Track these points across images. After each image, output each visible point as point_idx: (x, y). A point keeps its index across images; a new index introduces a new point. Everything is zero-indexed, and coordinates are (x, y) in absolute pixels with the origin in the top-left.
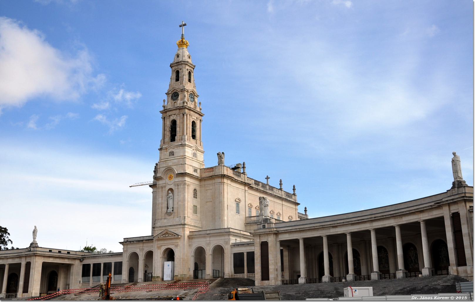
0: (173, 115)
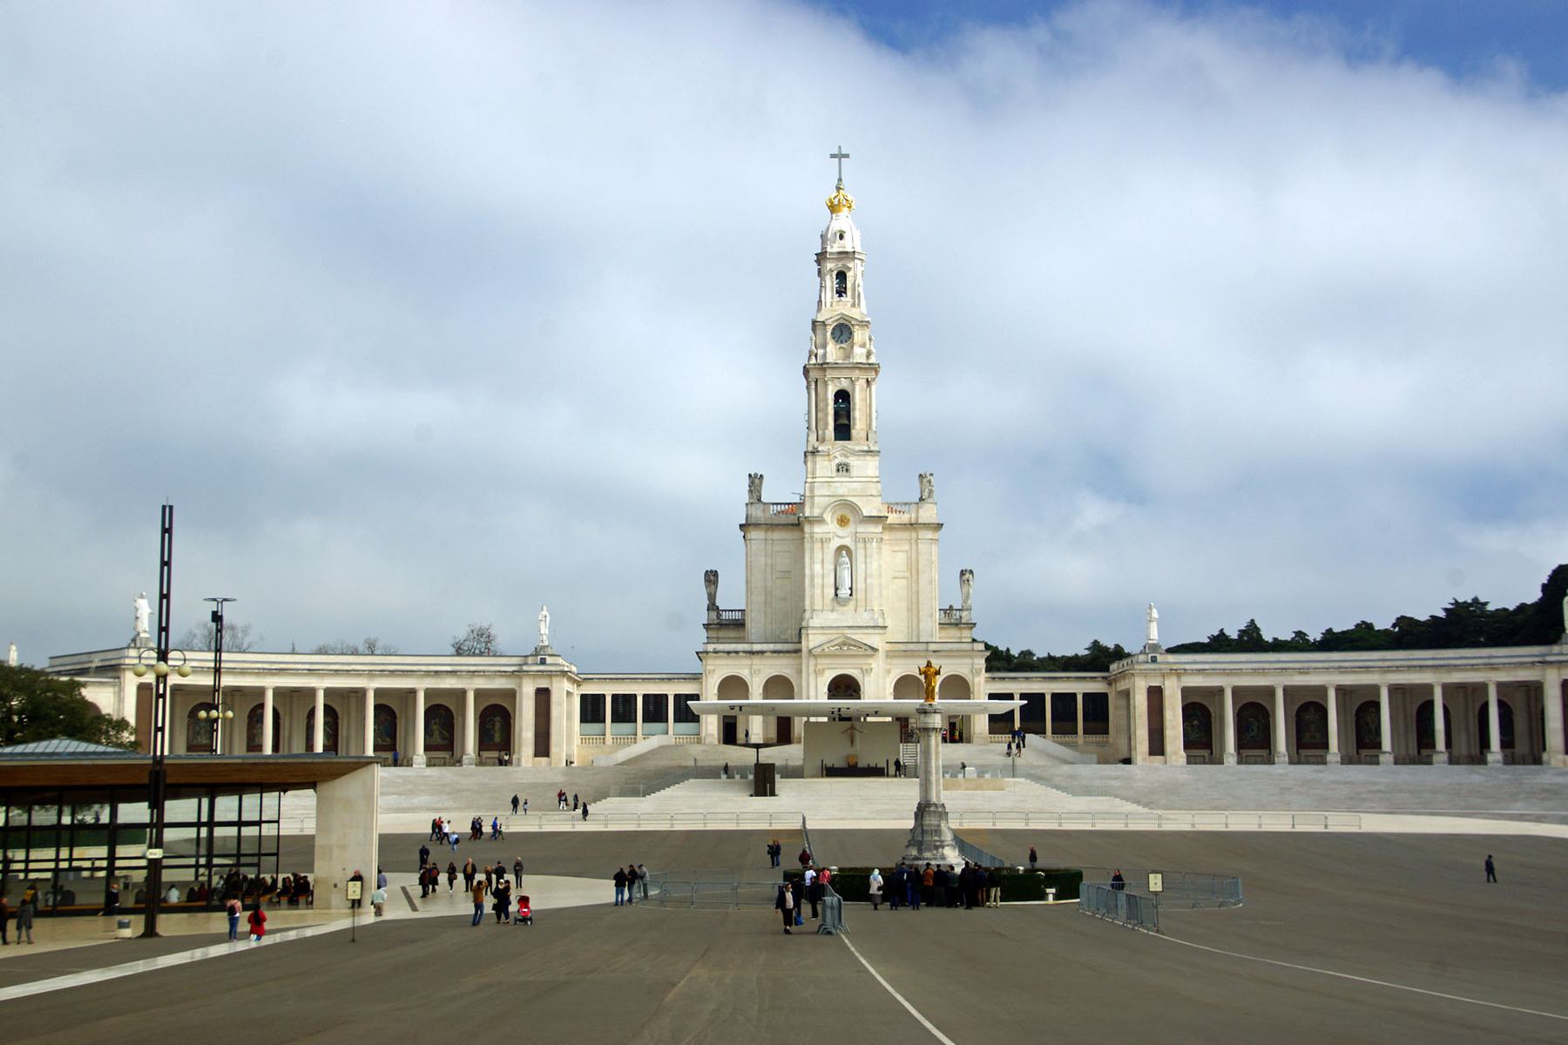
0: (842, 379)
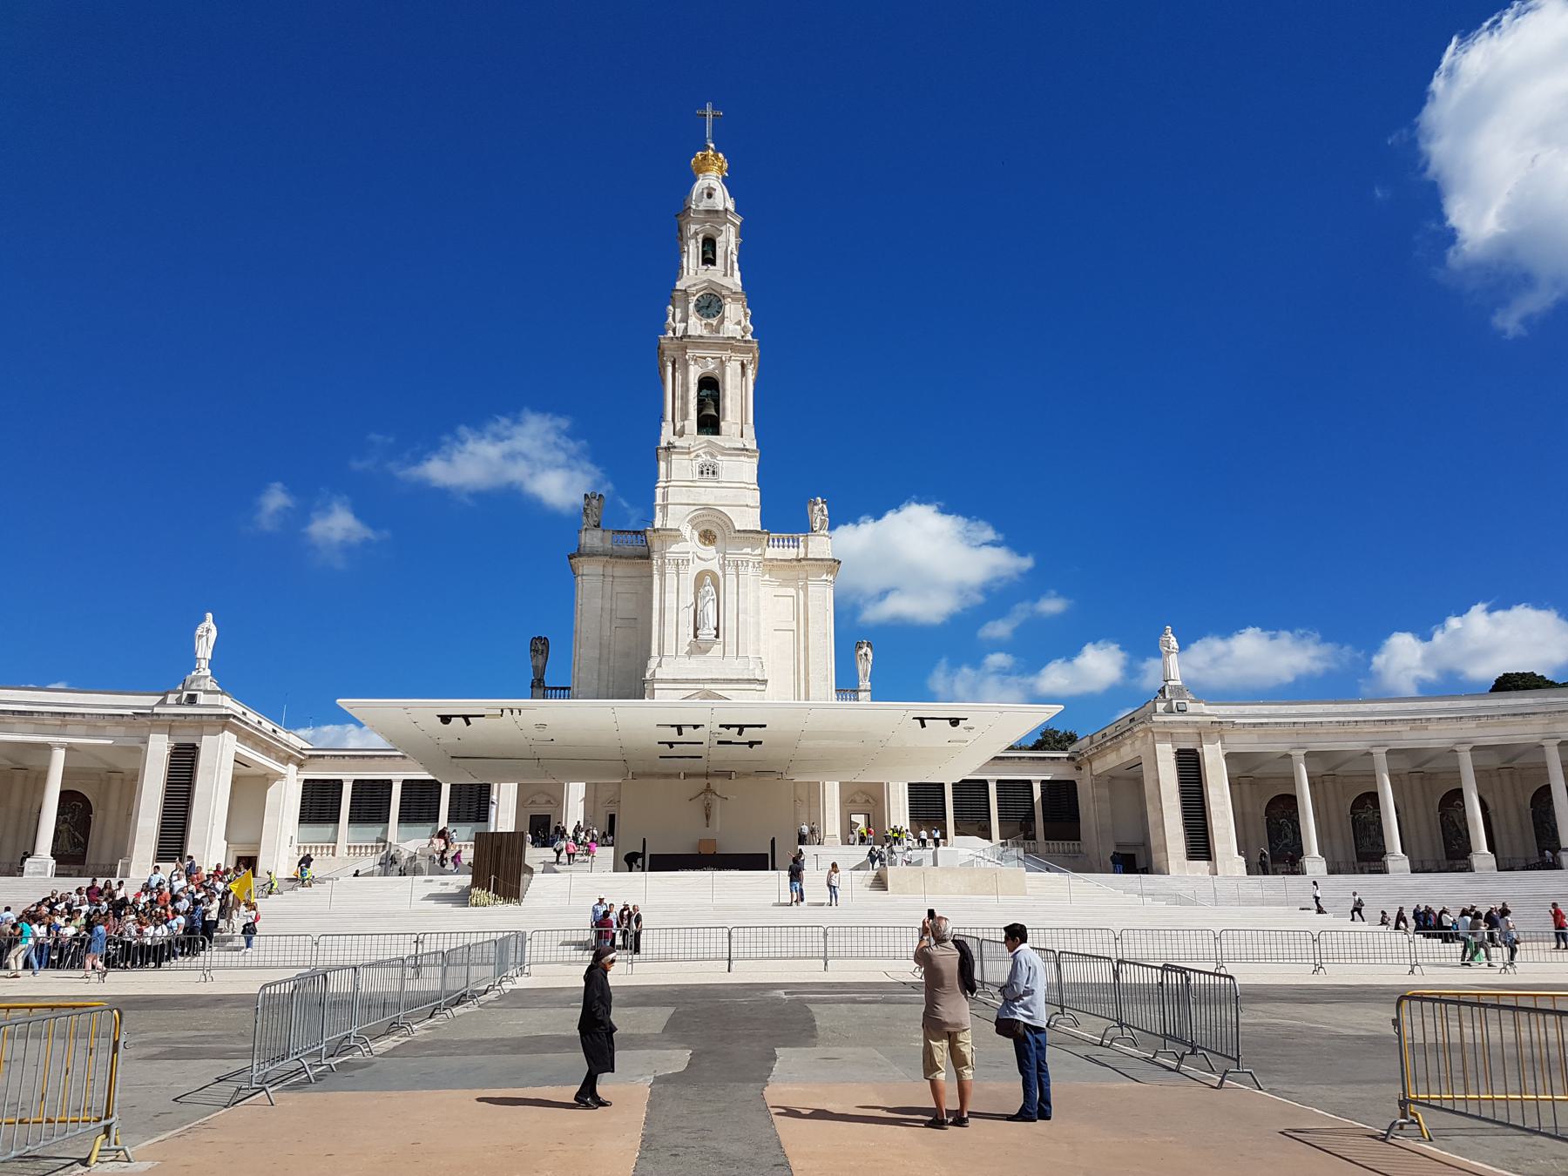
0: (709, 359)
